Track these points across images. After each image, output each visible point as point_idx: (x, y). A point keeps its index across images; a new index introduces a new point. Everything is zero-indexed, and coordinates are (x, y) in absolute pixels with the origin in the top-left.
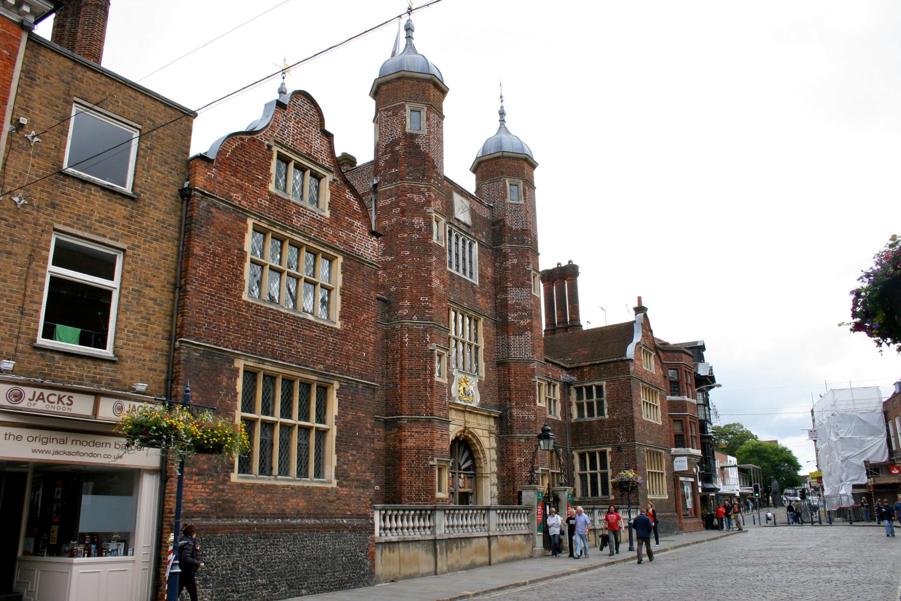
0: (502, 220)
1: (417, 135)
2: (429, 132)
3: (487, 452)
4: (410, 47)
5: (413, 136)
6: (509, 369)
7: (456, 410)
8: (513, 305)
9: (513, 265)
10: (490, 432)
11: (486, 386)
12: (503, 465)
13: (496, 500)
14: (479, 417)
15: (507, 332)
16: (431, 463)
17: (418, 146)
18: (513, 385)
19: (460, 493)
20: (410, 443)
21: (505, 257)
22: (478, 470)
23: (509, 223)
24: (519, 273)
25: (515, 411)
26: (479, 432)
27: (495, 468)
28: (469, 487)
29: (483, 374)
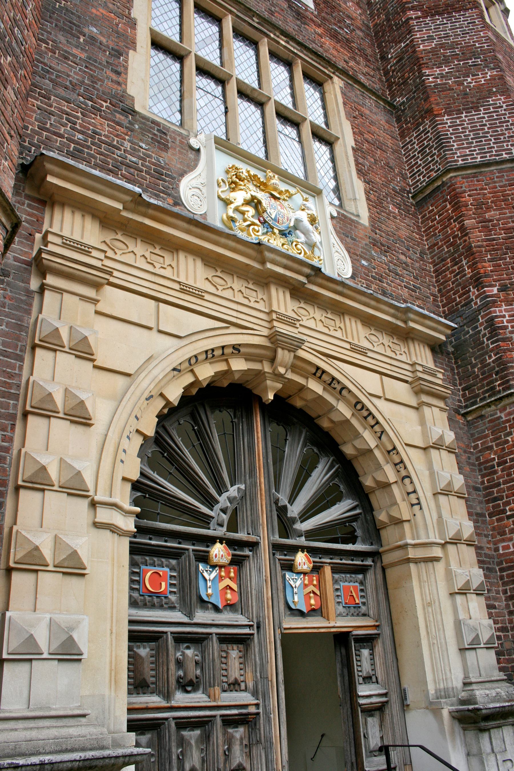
3: (415, 461)
6: (457, 206)
8: (433, 51)
12: (497, 512)
13: (486, 660)
15: (430, 111)
18: (477, 237)
19: (290, 642)
22: (389, 536)
26: (364, 382)
27: (459, 520)
28: (354, 609)
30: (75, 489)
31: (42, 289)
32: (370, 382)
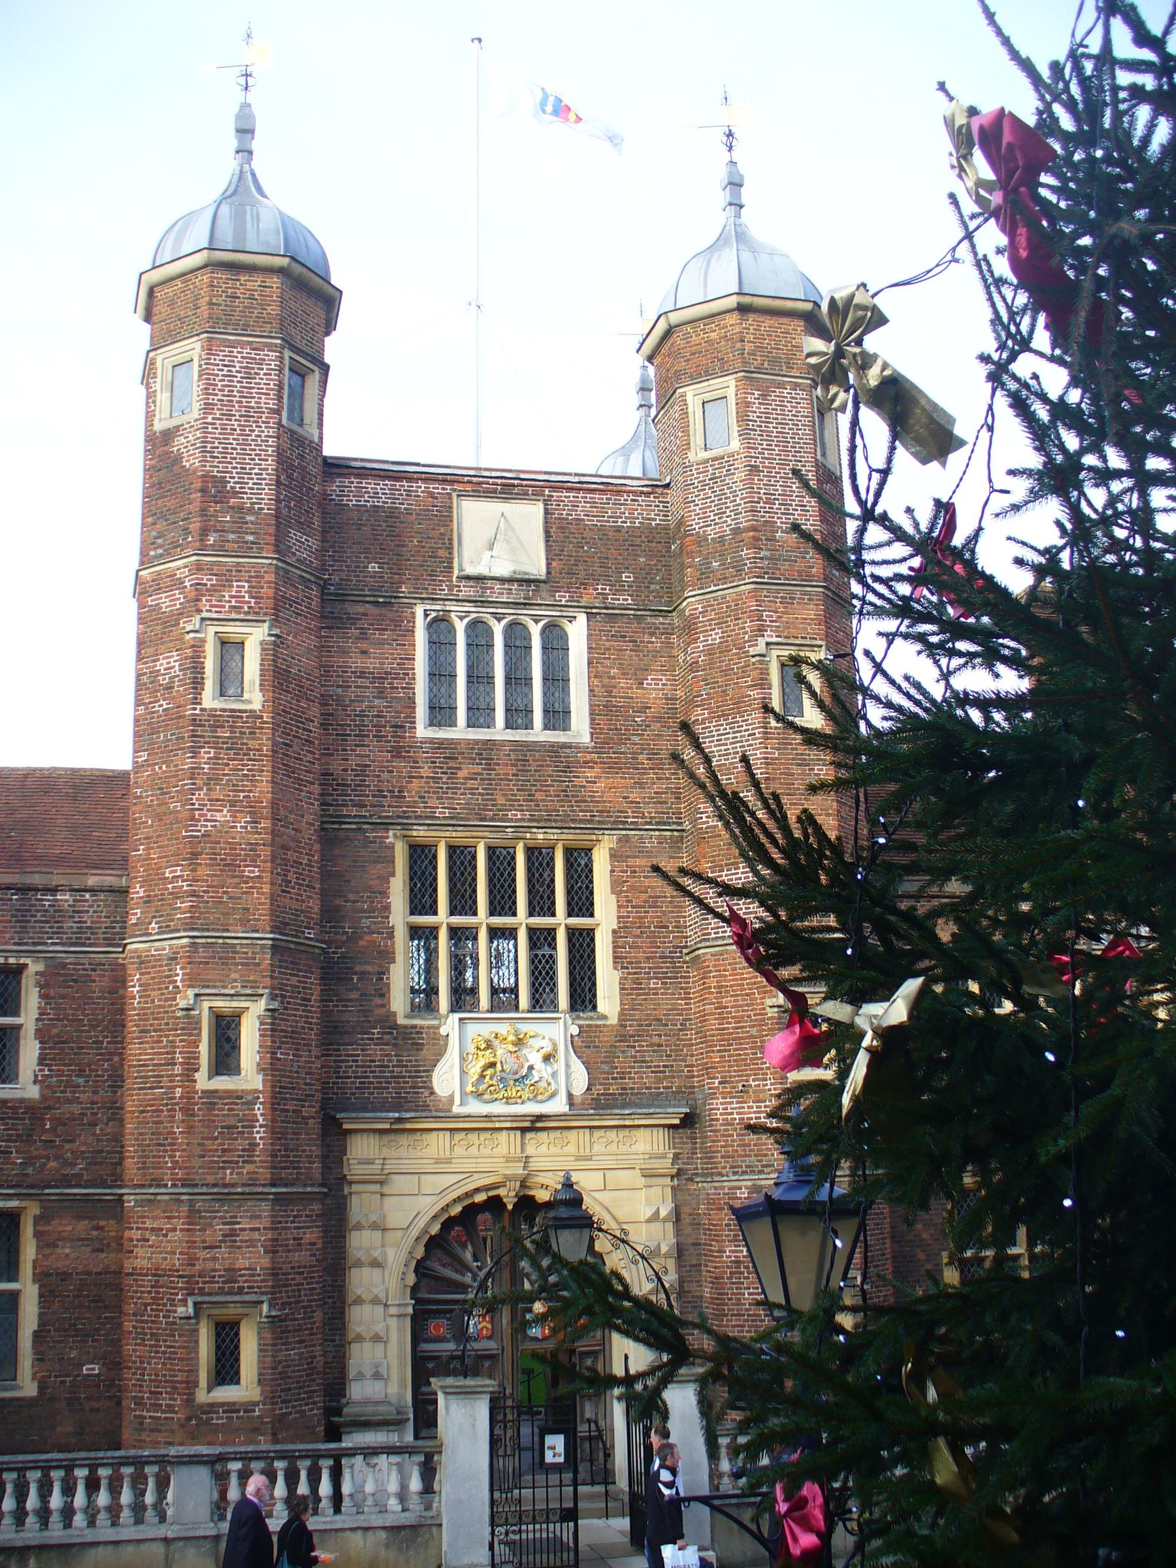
0: (681, 523)
1: (177, 428)
2: (208, 408)
5: (168, 436)
9: (710, 652)
11: (623, 1038)
16: (181, 1310)
17: (178, 458)
20: (142, 1259)
21: (690, 628)
23: (695, 525)
24: (726, 672)
25: (718, 1103)
30: (375, 1301)
31: (351, 1194)
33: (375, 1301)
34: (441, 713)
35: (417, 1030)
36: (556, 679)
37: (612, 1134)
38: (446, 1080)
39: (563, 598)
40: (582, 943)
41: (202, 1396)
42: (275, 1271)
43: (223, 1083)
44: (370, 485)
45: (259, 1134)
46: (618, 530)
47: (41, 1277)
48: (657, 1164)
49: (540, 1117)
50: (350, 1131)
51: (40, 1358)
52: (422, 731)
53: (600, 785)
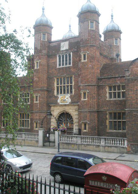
4: (43, 15)
7: (59, 106)
10: (76, 110)
14: (70, 106)
29: (73, 93)
32: (71, 111)
33: (53, 122)
34: (60, 65)
35: (57, 96)
36: (70, 60)
37: (73, 106)
38: (59, 101)
39: (70, 51)
40: (71, 86)
41: (35, 129)
42: (39, 119)
43: (36, 102)
44: (54, 43)
45: (38, 106)
46: (75, 42)
47: (30, 119)
48: (76, 109)
49: (65, 104)
50: (51, 106)
51: (30, 125)
52: (58, 67)
53: (72, 70)
